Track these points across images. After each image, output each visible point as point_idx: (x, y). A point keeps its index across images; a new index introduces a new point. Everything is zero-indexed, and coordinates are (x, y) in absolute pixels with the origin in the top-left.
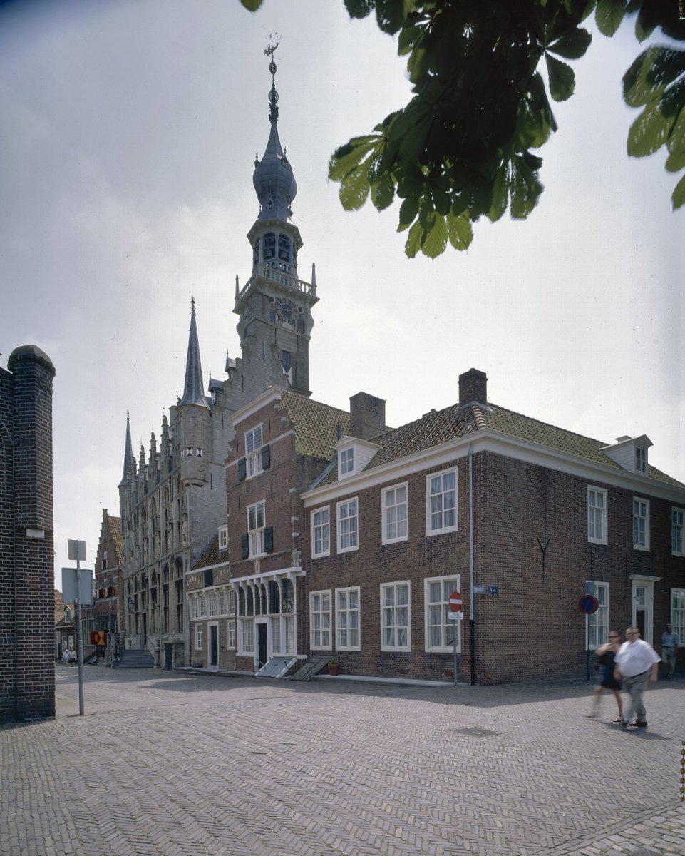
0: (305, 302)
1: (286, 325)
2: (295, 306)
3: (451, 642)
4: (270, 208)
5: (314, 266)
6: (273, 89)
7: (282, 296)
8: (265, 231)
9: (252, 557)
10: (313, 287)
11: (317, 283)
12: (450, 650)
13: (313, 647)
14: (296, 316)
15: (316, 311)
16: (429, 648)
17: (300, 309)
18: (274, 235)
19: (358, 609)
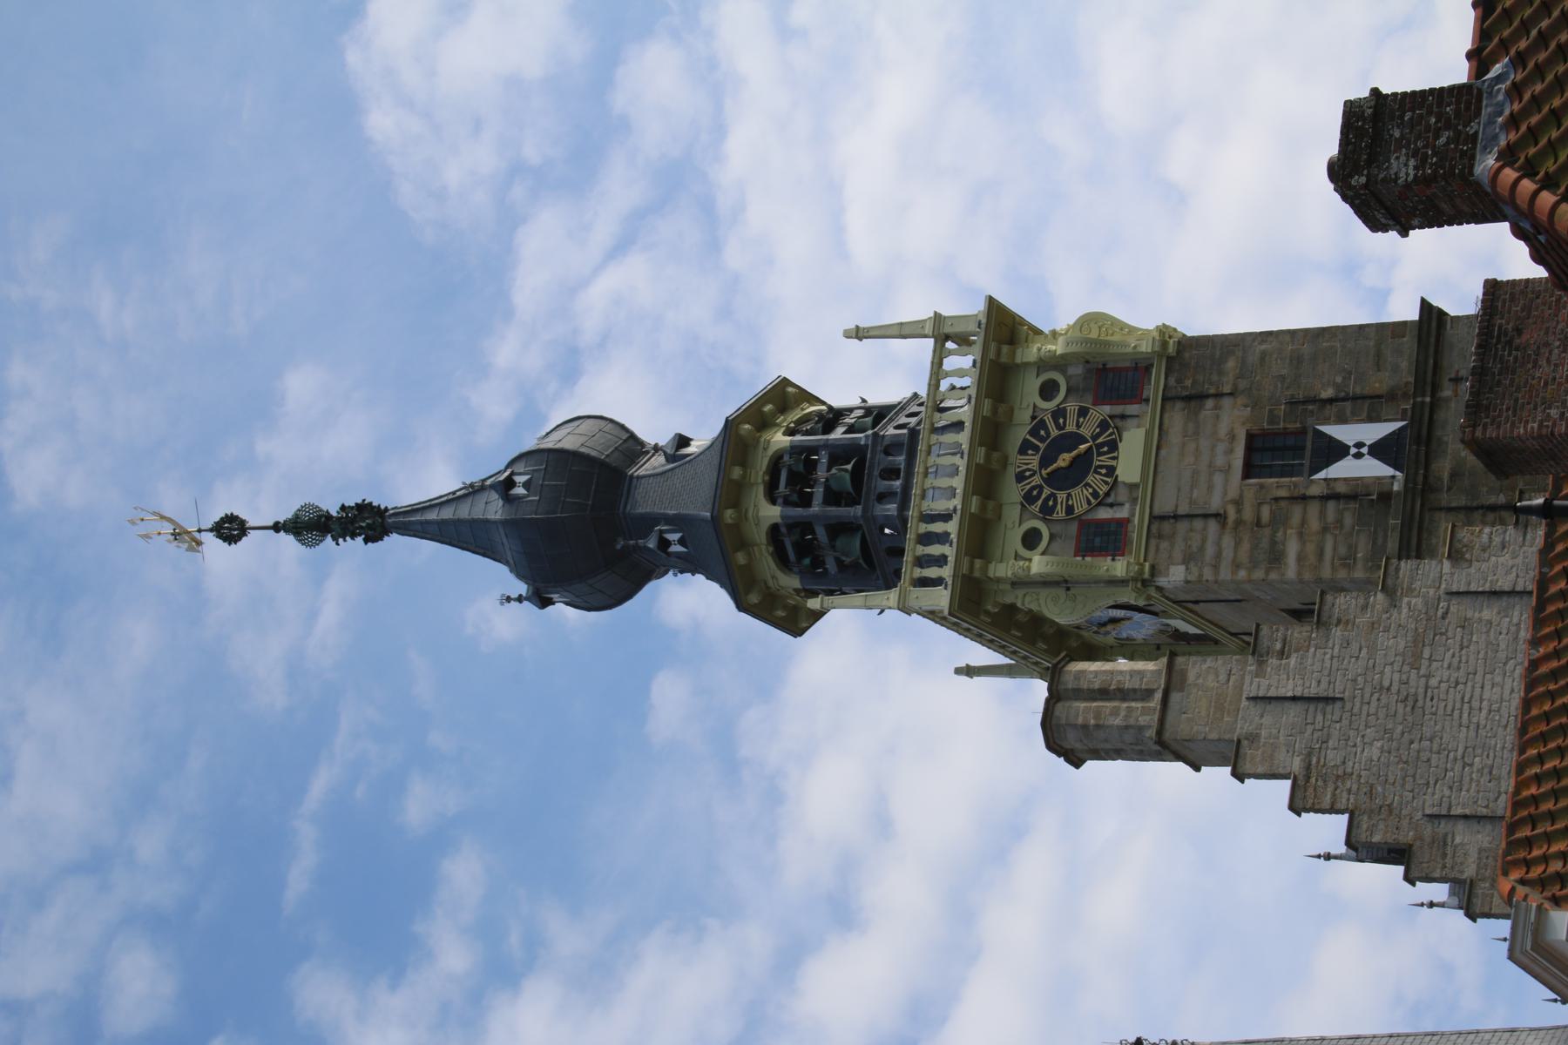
0: (1018, 366)
2: (1038, 427)
4: (681, 542)
5: (859, 334)
6: (276, 527)
7: (1013, 493)
8: (767, 565)
14: (1083, 412)
17: (1048, 390)
18: (774, 530)
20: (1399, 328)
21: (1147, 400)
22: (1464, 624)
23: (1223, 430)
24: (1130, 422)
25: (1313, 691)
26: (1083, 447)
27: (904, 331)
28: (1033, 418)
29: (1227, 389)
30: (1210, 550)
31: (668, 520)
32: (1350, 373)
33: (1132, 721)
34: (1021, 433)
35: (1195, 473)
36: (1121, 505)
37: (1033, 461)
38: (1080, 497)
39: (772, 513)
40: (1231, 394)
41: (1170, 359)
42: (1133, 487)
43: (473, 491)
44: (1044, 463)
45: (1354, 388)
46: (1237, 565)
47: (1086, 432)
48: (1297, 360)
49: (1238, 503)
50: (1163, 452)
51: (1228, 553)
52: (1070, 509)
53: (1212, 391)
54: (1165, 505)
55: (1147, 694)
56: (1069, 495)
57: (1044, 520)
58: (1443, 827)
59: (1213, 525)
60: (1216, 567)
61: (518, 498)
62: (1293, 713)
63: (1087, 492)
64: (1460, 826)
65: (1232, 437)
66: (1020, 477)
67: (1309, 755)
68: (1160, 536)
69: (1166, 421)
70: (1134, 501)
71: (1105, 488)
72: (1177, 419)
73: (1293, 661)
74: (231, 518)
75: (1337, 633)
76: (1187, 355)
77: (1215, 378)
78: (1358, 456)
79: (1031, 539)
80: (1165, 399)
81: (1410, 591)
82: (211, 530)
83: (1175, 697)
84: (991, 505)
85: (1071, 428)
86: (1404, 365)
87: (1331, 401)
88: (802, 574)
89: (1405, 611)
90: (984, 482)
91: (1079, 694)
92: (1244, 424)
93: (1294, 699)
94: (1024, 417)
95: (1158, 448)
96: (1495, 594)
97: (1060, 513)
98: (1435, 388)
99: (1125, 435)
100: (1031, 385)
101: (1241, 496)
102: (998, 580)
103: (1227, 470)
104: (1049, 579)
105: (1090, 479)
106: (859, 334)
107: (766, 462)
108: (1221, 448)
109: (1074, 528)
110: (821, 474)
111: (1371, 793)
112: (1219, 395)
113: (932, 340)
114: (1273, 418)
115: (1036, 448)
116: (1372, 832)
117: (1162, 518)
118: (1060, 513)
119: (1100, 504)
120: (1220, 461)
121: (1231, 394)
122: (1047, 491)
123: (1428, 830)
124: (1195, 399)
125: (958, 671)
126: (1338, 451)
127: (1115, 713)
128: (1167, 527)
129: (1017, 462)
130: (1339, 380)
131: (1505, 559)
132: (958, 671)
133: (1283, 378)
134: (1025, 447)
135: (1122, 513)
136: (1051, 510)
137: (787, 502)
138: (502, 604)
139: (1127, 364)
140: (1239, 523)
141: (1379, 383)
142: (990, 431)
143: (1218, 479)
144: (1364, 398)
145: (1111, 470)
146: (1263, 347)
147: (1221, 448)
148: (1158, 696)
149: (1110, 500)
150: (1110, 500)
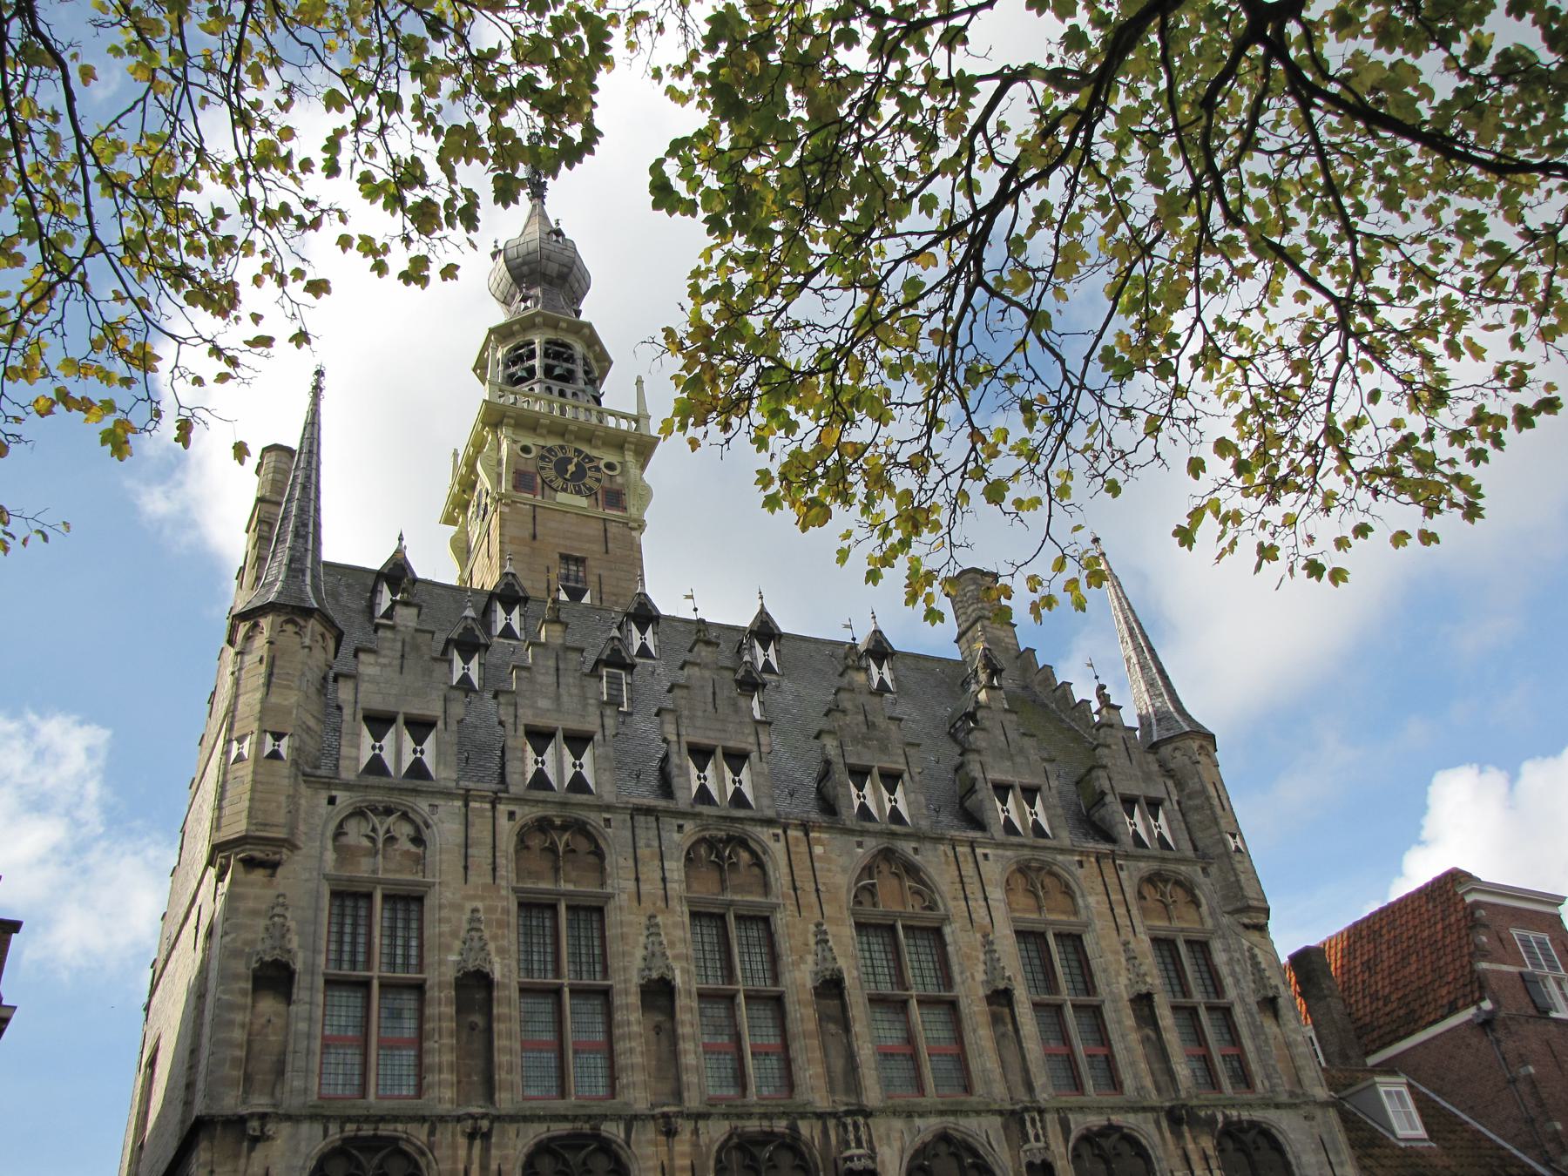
2: (591, 459)
7: (552, 442)
17: (610, 466)
34: (586, 449)
38: (550, 474)
79: (526, 449)
84: (544, 431)
85: (589, 474)
94: (594, 453)
97: (541, 464)
100: (612, 458)
106: (639, 382)
109: (532, 469)
118: (541, 464)
142: (589, 436)
145: (564, 490)
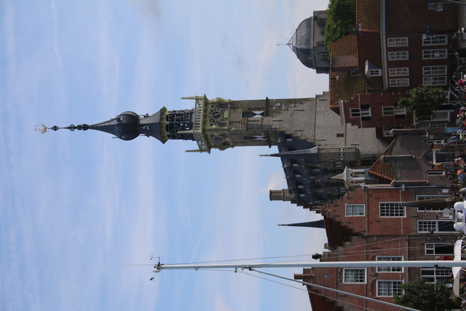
1: (226, 114)
2: (212, 111)
3: (444, 37)
4: (149, 128)
6: (65, 128)
7: (208, 119)
9: (405, 113)
10: (197, 99)
11: (194, 95)
12: (447, 38)
13: (446, 84)
14: (218, 109)
15: (212, 97)
16: (446, 44)
17: (213, 107)
18: (167, 125)
19: (431, 67)
20: (263, 100)
21: (228, 108)
22: (296, 113)
23: (239, 112)
24: (225, 111)
25: (280, 120)
26: (219, 114)
27: (190, 98)
28: (211, 110)
29: (239, 107)
30: (238, 126)
31: (147, 124)
32: (256, 105)
33: (257, 123)
34: (209, 112)
35: (235, 117)
36: (225, 120)
37: (211, 115)
38: (219, 120)
39: (168, 122)
40: (240, 108)
41: (231, 103)
42: (226, 118)
43: (113, 120)
44: (213, 115)
45: (257, 107)
46: (242, 128)
47: (219, 111)
48: (249, 104)
49: (242, 120)
50: (230, 114)
51: (241, 126)
52: (217, 121)
53: (237, 107)
54: (231, 121)
55: (259, 121)
56: (217, 119)
57: (214, 122)
58: (296, 132)
59: (238, 124)
60: (239, 128)
61: (122, 121)
62: (277, 122)
63: (220, 119)
64: (298, 131)
65: (240, 113)
66: (209, 117)
67: (280, 126)
68: (231, 124)
69: (231, 111)
70: (227, 120)
71: (222, 118)
72: (232, 110)
73: (277, 117)
74: (55, 127)
75: (282, 114)
76: (233, 103)
77: (237, 106)
78: (258, 115)
80: (230, 108)
81: (290, 110)
82: (51, 128)
83: (263, 121)
85: (217, 111)
86: (264, 105)
87: (254, 108)
88: (170, 132)
89: (289, 112)
90: (205, 116)
91: (250, 121)
92: (242, 111)
93: (277, 121)
95: (230, 114)
96: (300, 110)
97: (216, 121)
98: (268, 107)
99: (225, 112)
101: (242, 119)
102: (207, 129)
103: (240, 116)
104: (215, 129)
105: (220, 117)
107: (166, 116)
108: (239, 114)
109: (218, 123)
110: (175, 117)
111: (287, 129)
112: (238, 108)
113: (195, 100)
114: (246, 110)
115: (212, 113)
116: (288, 132)
117: (231, 122)
118: (216, 121)
119: (221, 120)
120: (239, 115)
121: (240, 108)
122: (214, 119)
123: (294, 132)
124: (234, 108)
125: (186, 151)
126: (255, 114)
127: (255, 123)
128: (231, 123)
129: (208, 115)
130: (255, 106)
131: (300, 107)
132: (186, 151)
133: (247, 106)
134: (210, 113)
135: (225, 122)
136: (215, 121)
137: (170, 121)
138: (113, 138)
139: (224, 104)
140: (242, 123)
141: (260, 107)
142: (205, 111)
143: (239, 118)
144: (258, 108)
145: (223, 116)
146: (244, 102)
147: (239, 114)
148: (261, 121)
149: (223, 120)
150: (223, 120)
